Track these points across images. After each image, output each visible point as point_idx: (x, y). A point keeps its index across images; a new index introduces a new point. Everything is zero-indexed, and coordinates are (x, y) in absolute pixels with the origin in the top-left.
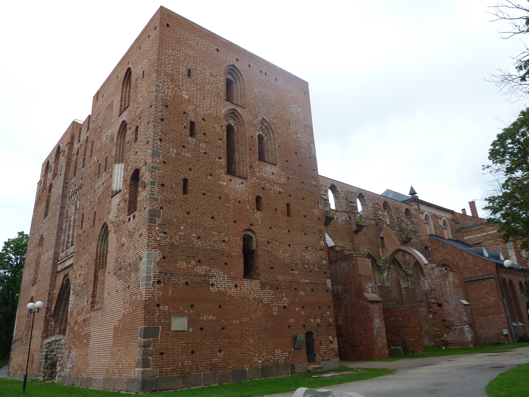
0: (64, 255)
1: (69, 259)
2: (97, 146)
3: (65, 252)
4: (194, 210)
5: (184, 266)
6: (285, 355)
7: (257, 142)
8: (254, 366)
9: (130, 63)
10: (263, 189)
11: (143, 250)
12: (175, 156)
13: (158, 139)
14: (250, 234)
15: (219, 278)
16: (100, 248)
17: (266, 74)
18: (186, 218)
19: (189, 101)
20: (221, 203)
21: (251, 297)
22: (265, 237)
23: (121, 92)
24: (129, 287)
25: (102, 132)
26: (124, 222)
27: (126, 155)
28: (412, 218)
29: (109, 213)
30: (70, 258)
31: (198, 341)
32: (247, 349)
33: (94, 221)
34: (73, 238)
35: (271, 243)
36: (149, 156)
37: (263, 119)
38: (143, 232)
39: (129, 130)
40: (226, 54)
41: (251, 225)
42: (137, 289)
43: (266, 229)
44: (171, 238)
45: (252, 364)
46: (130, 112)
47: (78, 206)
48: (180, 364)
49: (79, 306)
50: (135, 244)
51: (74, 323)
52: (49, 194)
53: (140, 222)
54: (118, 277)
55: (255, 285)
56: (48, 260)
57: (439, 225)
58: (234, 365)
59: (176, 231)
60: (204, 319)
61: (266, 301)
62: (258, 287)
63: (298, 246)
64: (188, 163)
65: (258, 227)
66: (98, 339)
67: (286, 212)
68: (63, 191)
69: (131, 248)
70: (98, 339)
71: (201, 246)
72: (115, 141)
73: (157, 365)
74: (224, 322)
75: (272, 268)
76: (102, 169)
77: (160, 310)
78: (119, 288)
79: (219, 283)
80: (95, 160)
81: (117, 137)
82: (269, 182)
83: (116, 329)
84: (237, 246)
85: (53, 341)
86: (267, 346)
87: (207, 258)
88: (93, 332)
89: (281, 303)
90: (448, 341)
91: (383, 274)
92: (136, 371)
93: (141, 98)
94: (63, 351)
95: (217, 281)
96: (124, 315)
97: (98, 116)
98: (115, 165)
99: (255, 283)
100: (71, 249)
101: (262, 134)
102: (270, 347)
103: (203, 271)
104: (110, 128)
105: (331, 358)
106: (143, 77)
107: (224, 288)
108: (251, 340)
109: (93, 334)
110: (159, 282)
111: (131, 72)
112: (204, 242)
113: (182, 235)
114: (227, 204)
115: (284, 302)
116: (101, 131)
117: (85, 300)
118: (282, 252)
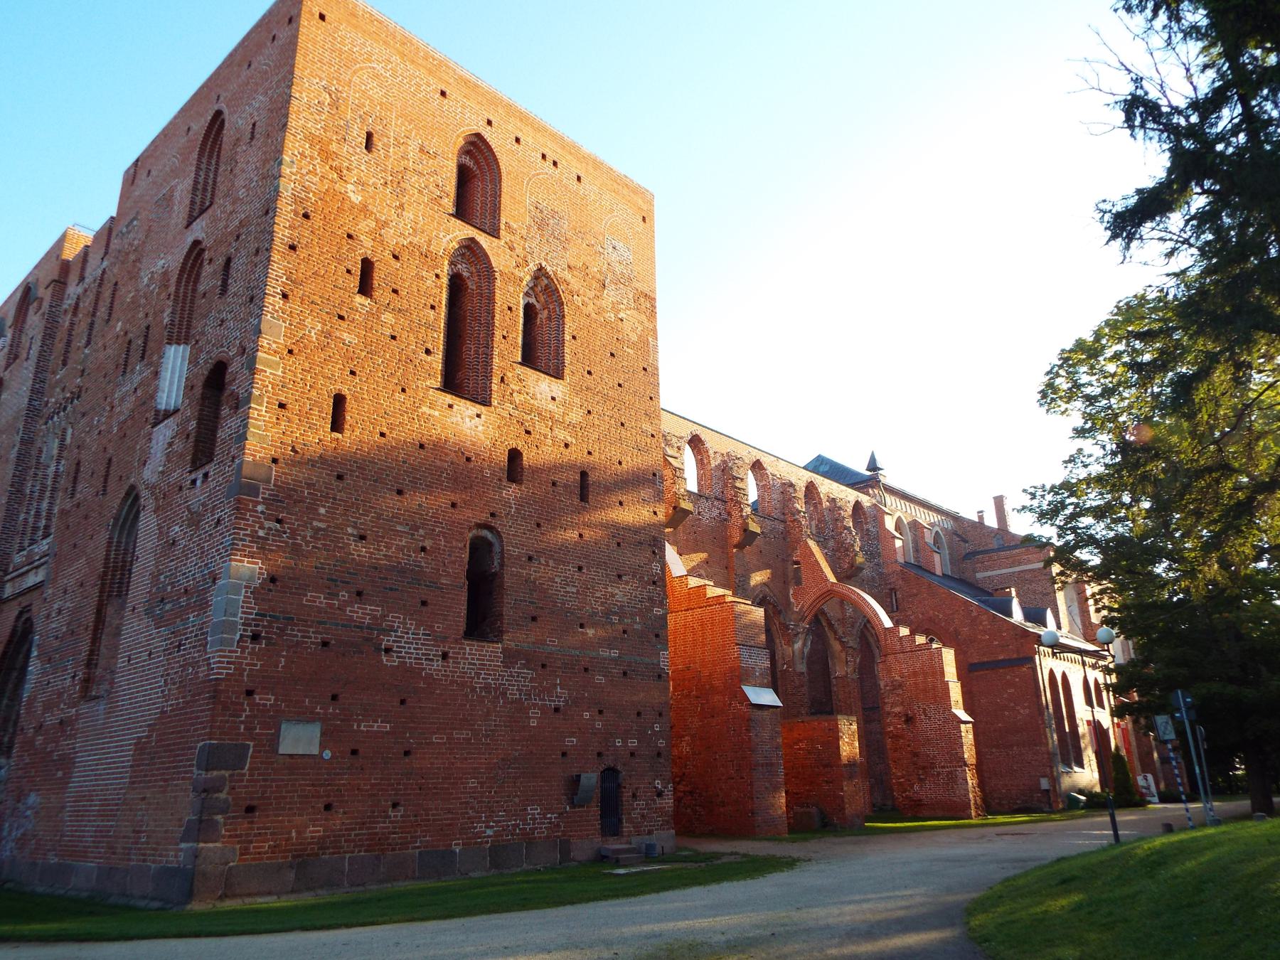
0: (24, 559)
1: (34, 571)
2: (126, 294)
3: (25, 553)
4: (355, 471)
5: (321, 603)
6: (551, 818)
8: (476, 843)
9: (222, 99)
11: (220, 559)
12: (317, 339)
13: (278, 294)
14: (486, 533)
15: (406, 636)
16: (116, 546)
17: (555, 164)
18: (333, 489)
19: (364, 209)
20: (421, 459)
21: (478, 683)
22: (523, 545)
23: (194, 169)
24: (180, 645)
25: (141, 263)
26: (181, 488)
27: (198, 326)
28: (866, 524)
29: (144, 464)
30: (37, 567)
32: (461, 803)
33: (106, 481)
34: (50, 520)
36: (252, 333)
37: (541, 269)
38: (225, 514)
39: (209, 263)
40: (463, 107)
41: (493, 515)
42: (198, 651)
43: (527, 526)
44: (294, 534)
45: (470, 838)
46: (215, 220)
47: (68, 440)
48: (294, 834)
49: (53, 687)
50: (204, 543)
51: (34, 728)
53: (219, 490)
54: (156, 620)
55: (490, 656)
57: (925, 542)
59: (305, 519)
60: (362, 728)
61: (513, 694)
63: (599, 570)
65: (508, 522)
66: (92, 770)
67: (577, 491)
68: (30, 400)
69: (192, 552)
70: (92, 770)
71: (365, 557)
72: (172, 289)
73: (236, 836)
74: (410, 738)
76: (135, 355)
77: (253, 705)
78: (155, 648)
79: (404, 648)
80: (118, 329)
81: (178, 278)
83: (140, 747)
84: (454, 563)
86: (509, 796)
87: (378, 587)
88: (81, 751)
89: (549, 701)
90: (920, 800)
91: (793, 643)
92: (181, 850)
93: (243, 190)
95: (400, 642)
96: (163, 712)
97: (135, 223)
98: (168, 346)
99: (492, 652)
100: (44, 546)
101: (536, 303)
102: (517, 800)
104: (162, 255)
105: (657, 830)
106: (252, 138)
107: (416, 659)
108: (472, 783)
109: (82, 757)
110: (255, 637)
111: (223, 122)
112: (374, 549)
113: (320, 529)
115: (557, 697)
116: (138, 260)
117: (69, 674)
118: (560, 583)
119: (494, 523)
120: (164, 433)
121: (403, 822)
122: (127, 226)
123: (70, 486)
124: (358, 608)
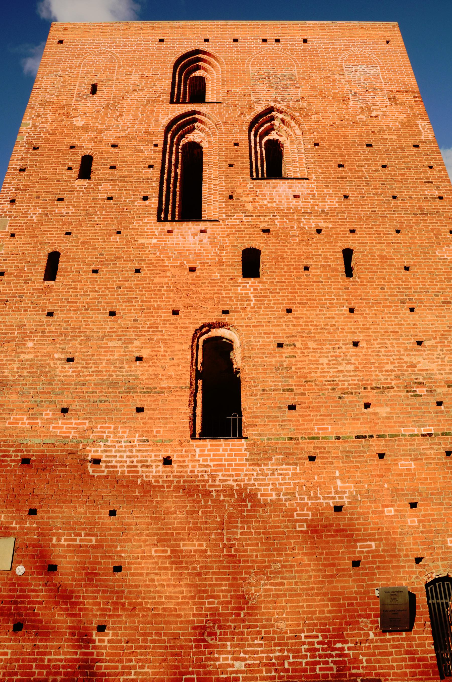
19: (86, 127)
31: (38, 597)
35: (287, 345)
41: (226, 312)
58: (146, 670)
60: (62, 542)
62: (241, 460)
63: (386, 341)
71: (73, 376)
74: (121, 551)
75: (292, 407)
79: (115, 456)
89: (324, 498)
99: (231, 450)
103: (73, 431)
118: (328, 364)
119: (226, 319)
121: (112, 648)
124: (62, 423)
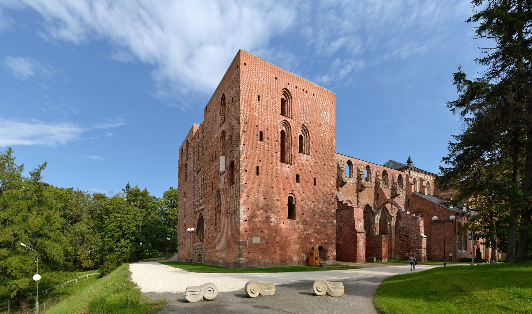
7: (299, 140)
10: (301, 170)
24: (232, 222)
47: (203, 177)
52: (186, 169)
56: (190, 206)
64: (259, 157)
72: (220, 142)
82: (304, 166)
83: (228, 241)
85: (198, 245)
94: (203, 250)
97: (209, 124)
98: (221, 157)
110: (246, 220)
114: (280, 180)
120: (223, 177)
122: (207, 125)
123: (205, 188)
